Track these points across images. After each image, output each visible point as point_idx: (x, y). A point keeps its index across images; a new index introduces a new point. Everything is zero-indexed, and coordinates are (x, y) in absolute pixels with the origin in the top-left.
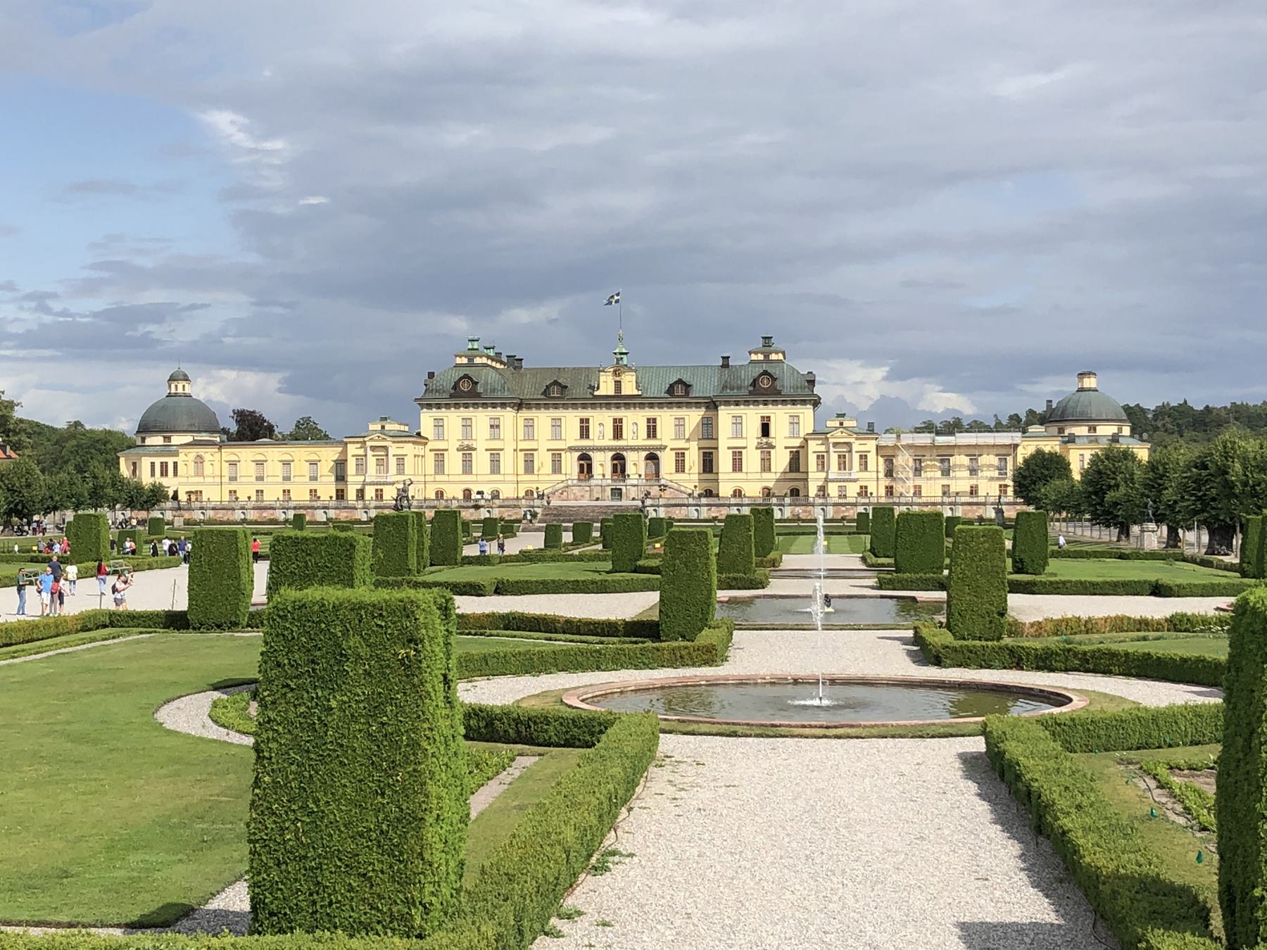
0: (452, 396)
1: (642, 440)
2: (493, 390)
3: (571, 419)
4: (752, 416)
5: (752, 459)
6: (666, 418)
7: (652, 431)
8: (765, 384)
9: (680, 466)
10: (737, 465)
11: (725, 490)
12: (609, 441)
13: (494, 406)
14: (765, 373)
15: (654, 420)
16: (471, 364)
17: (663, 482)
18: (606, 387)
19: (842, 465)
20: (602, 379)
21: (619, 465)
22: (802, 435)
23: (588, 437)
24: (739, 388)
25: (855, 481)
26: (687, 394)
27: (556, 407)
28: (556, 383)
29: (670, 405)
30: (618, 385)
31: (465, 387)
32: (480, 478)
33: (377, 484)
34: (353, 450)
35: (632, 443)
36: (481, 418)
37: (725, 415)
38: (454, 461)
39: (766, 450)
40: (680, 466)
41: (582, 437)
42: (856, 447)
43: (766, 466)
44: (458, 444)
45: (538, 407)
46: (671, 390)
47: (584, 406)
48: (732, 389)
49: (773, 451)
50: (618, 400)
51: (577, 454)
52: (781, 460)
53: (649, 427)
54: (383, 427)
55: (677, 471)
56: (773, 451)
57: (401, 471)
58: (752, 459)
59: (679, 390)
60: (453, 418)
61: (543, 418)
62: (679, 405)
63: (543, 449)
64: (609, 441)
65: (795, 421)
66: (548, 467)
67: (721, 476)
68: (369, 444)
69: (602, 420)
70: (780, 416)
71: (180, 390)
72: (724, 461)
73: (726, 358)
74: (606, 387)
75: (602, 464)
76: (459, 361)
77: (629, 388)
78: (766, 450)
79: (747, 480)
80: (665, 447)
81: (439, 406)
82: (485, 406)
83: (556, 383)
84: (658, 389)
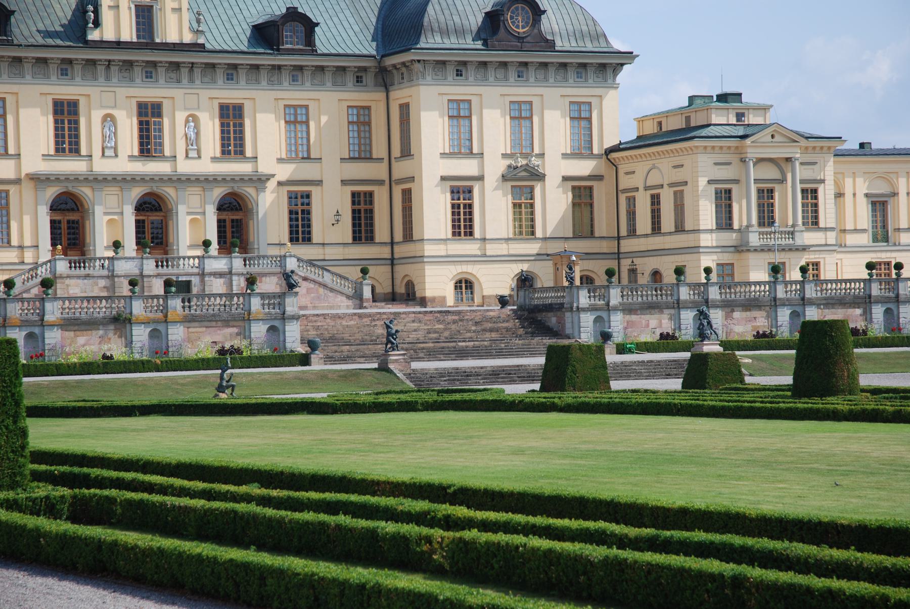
5: (494, 210)
9: (300, 228)
10: (463, 222)
12: (124, 161)
19: (766, 217)
21: (153, 222)
23: (75, 150)
24: (460, 32)
25: (804, 249)
39: (523, 179)
40: (300, 228)
41: (59, 150)
42: (801, 172)
43: (525, 223)
46: (266, 34)
48: (445, 32)
51: (51, 192)
55: (294, 239)
58: (494, 210)
64: (124, 161)
65: (581, 116)
67: (429, 250)
72: (434, 213)
75: (111, 223)
78: (523, 179)
79: (484, 258)
80: (269, 177)
84: (230, 34)
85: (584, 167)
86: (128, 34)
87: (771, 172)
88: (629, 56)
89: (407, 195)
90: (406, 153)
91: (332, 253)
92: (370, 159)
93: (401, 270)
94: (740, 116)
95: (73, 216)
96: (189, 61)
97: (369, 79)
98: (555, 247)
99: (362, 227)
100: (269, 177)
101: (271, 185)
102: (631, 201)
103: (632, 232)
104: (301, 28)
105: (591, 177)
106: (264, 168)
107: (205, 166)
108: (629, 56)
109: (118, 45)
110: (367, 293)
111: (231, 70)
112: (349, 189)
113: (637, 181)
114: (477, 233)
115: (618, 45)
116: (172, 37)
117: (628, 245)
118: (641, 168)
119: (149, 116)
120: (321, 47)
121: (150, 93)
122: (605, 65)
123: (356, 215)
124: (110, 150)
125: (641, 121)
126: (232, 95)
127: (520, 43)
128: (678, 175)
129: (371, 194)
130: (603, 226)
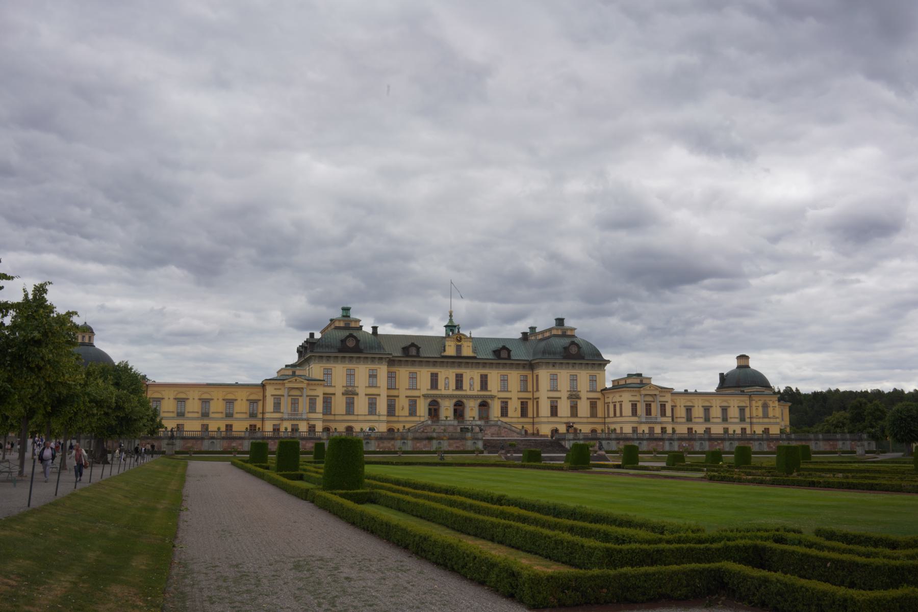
0: (340, 351)
1: (476, 390)
2: (372, 348)
3: (424, 374)
4: (564, 375)
5: (564, 409)
6: (494, 376)
8: (574, 350)
9: (504, 412)
10: (554, 411)
14: (573, 343)
15: (486, 376)
16: (347, 328)
17: (499, 423)
18: (451, 351)
20: (447, 344)
21: (459, 410)
22: (599, 390)
24: (554, 353)
25: (661, 423)
26: (509, 358)
27: (413, 363)
28: (413, 345)
29: (498, 366)
30: (459, 348)
31: (351, 343)
32: (360, 418)
33: (294, 420)
34: (270, 390)
35: (469, 393)
36: (362, 371)
37: (544, 374)
38: (339, 405)
39: (574, 397)
40: (504, 412)
46: (497, 353)
47: (435, 364)
48: (549, 353)
49: (579, 402)
50: (459, 360)
51: (429, 400)
52: (584, 408)
53: (482, 382)
54: (294, 373)
56: (579, 402)
58: (564, 409)
59: (504, 354)
60: (339, 371)
61: (403, 373)
65: (593, 380)
66: (406, 412)
68: (288, 385)
69: (447, 375)
70: (583, 376)
71: (87, 340)
73: (524, 334)
75: (447, 410)
76: (337, 324)
77: (467, 351)
87: (650, 399)
88: (609, 361)
89: (537, 402)
90: (537, 390)
92: (526, 391)
93: (536, 426)
94: (641, 381)
98: (566, 420)
99: (524, 413)
100: (495, 397)
101: (496, 400)
102: (608, 406)
103: (609, 417)
106: (494, 393)
107: (475, 393)
108: (609, 361)
110: (523, 432)
111: (484, 364)
113: (609, 400)
114: (559, 414)
115: (606, 357)
117: (607, 420)
118: (611, 396)
119: (459, 379)
120: (513, 358)
121: (459, 371)
124: (447, 387)
125: (613, 381)
126: (484, 372)
128: (620, 399)
130: (600, 413)
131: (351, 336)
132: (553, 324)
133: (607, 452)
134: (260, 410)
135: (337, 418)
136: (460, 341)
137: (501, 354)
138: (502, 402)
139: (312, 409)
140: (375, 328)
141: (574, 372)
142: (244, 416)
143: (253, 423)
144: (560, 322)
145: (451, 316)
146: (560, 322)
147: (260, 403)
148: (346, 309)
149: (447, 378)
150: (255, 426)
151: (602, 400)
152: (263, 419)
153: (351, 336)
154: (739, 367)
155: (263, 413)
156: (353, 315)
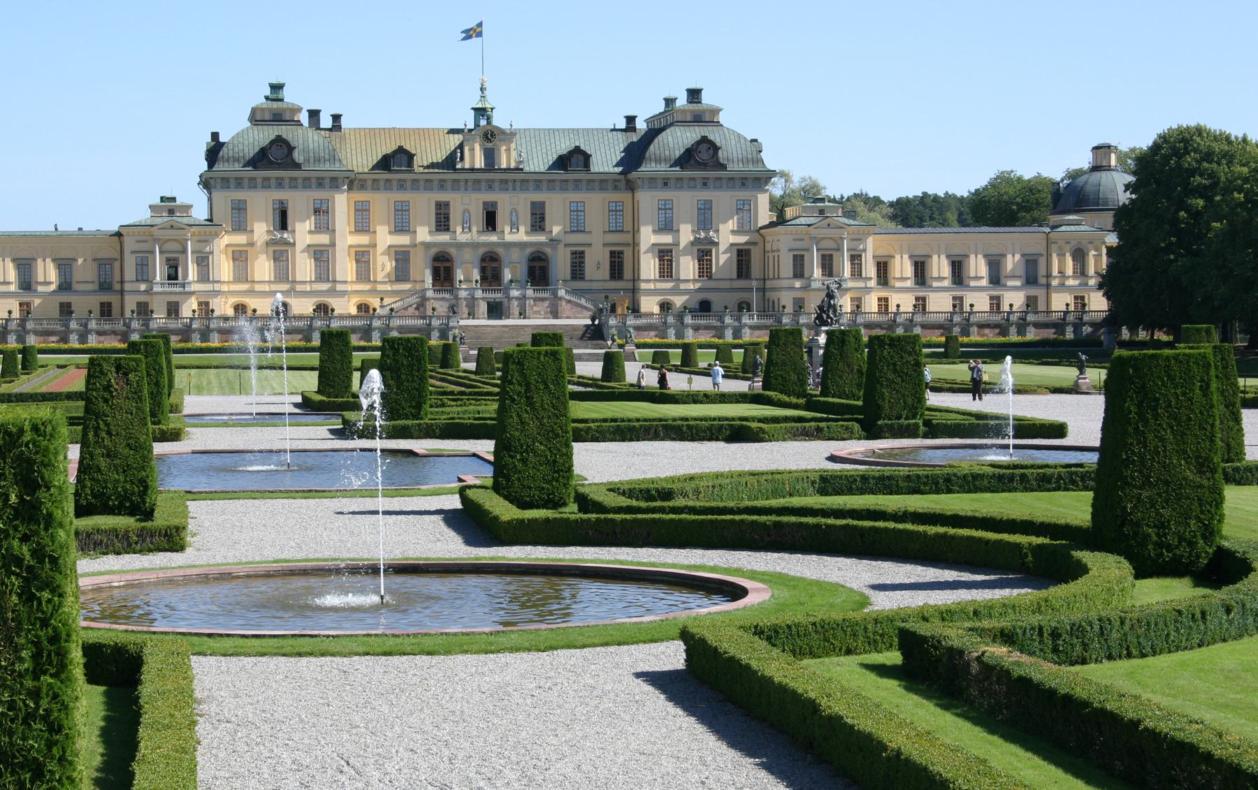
2: (318, 160)
4: (685, 201)
6: (557, 205)
7: (538, 222)
11: (650, 305)
13: (320, 184)
15: (542, 204)
27: (402, 186)
29: (564, 186)
30: (490, 155)
36: (299, 201)
37: (647, 200)
44: (266, 238)
45: (376, 185)
47: (442, 186)
57: (204, 277)
60: (261, 203)
62: (577, 186)
63: (381, 247)
69: (466, 204)
72: (649, 267)
73: (631, 120)
74: (475, 158)
81: (239, 183)
82: (307, 184)
83: (401, 150)
85: (742, 239)
86: (479, 162)
87: (832, 245)
91: (595, 286)
95: (447, 264)
96: (517, 179)
97: (622, 185)
99: (616, 270)
101: (561, 246)
104: (581, 158)
105: (746, 243)
109: (472, 170)
112: (608, 250)
116: (504, 166)
117: (769, 284)
122: (762, 179)
123: (612, 264)
126: (538, 197)
127: (703, 166)
129: (621, 253)
130: (756, 270)
131: (279, 141)
132: (682, 101)
133: (638, 346)
134: (117, 277)
135: (258, 288)
136: (489, 140)
137: (573, 161)
138: (574, 253)
139: (204, 277)
140: (336, 118)
141: (705, 195)
142: (90, 287)
143: (106, 298)
144: (694, 94)
145: (482, 89)
146: (694, 94)
147: (117, 265)
148: (277, 88)
149: (466, 211)
150: (110, 304)
151: (761, 244)
152: (122, 292)
153: (279, 141)
154: (1096, 168)
155: (122, 282)
156: (289, 96)
